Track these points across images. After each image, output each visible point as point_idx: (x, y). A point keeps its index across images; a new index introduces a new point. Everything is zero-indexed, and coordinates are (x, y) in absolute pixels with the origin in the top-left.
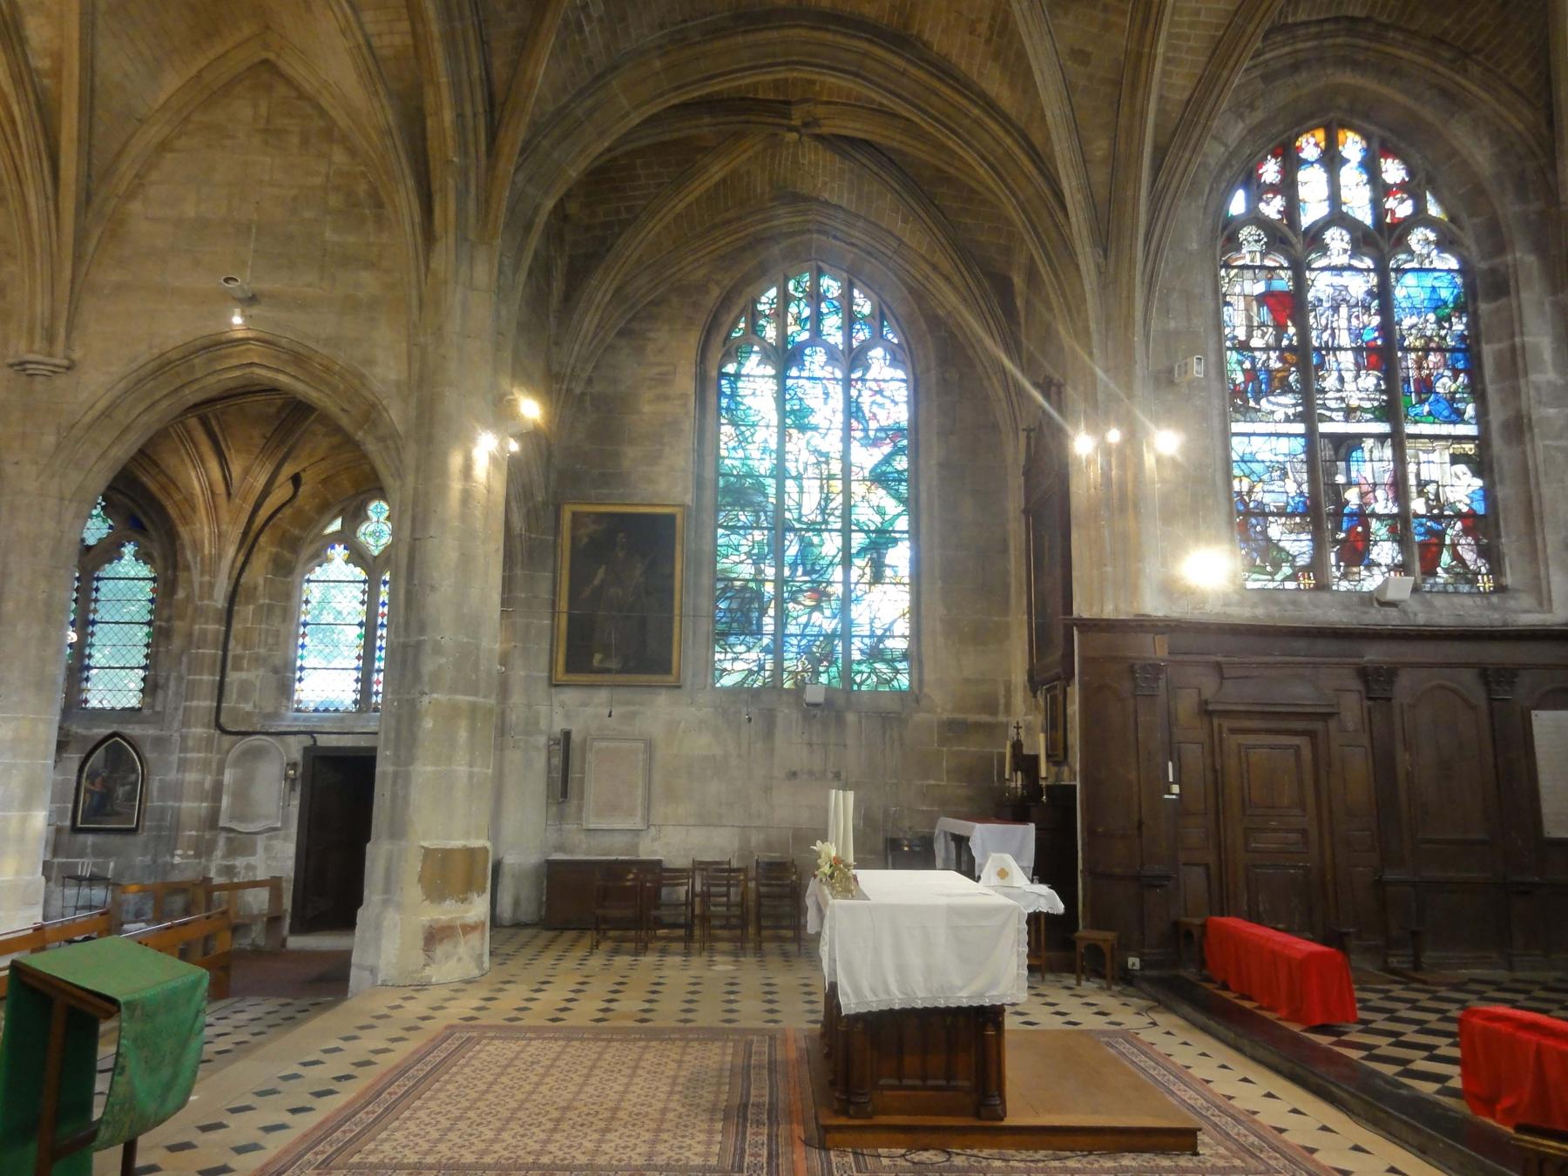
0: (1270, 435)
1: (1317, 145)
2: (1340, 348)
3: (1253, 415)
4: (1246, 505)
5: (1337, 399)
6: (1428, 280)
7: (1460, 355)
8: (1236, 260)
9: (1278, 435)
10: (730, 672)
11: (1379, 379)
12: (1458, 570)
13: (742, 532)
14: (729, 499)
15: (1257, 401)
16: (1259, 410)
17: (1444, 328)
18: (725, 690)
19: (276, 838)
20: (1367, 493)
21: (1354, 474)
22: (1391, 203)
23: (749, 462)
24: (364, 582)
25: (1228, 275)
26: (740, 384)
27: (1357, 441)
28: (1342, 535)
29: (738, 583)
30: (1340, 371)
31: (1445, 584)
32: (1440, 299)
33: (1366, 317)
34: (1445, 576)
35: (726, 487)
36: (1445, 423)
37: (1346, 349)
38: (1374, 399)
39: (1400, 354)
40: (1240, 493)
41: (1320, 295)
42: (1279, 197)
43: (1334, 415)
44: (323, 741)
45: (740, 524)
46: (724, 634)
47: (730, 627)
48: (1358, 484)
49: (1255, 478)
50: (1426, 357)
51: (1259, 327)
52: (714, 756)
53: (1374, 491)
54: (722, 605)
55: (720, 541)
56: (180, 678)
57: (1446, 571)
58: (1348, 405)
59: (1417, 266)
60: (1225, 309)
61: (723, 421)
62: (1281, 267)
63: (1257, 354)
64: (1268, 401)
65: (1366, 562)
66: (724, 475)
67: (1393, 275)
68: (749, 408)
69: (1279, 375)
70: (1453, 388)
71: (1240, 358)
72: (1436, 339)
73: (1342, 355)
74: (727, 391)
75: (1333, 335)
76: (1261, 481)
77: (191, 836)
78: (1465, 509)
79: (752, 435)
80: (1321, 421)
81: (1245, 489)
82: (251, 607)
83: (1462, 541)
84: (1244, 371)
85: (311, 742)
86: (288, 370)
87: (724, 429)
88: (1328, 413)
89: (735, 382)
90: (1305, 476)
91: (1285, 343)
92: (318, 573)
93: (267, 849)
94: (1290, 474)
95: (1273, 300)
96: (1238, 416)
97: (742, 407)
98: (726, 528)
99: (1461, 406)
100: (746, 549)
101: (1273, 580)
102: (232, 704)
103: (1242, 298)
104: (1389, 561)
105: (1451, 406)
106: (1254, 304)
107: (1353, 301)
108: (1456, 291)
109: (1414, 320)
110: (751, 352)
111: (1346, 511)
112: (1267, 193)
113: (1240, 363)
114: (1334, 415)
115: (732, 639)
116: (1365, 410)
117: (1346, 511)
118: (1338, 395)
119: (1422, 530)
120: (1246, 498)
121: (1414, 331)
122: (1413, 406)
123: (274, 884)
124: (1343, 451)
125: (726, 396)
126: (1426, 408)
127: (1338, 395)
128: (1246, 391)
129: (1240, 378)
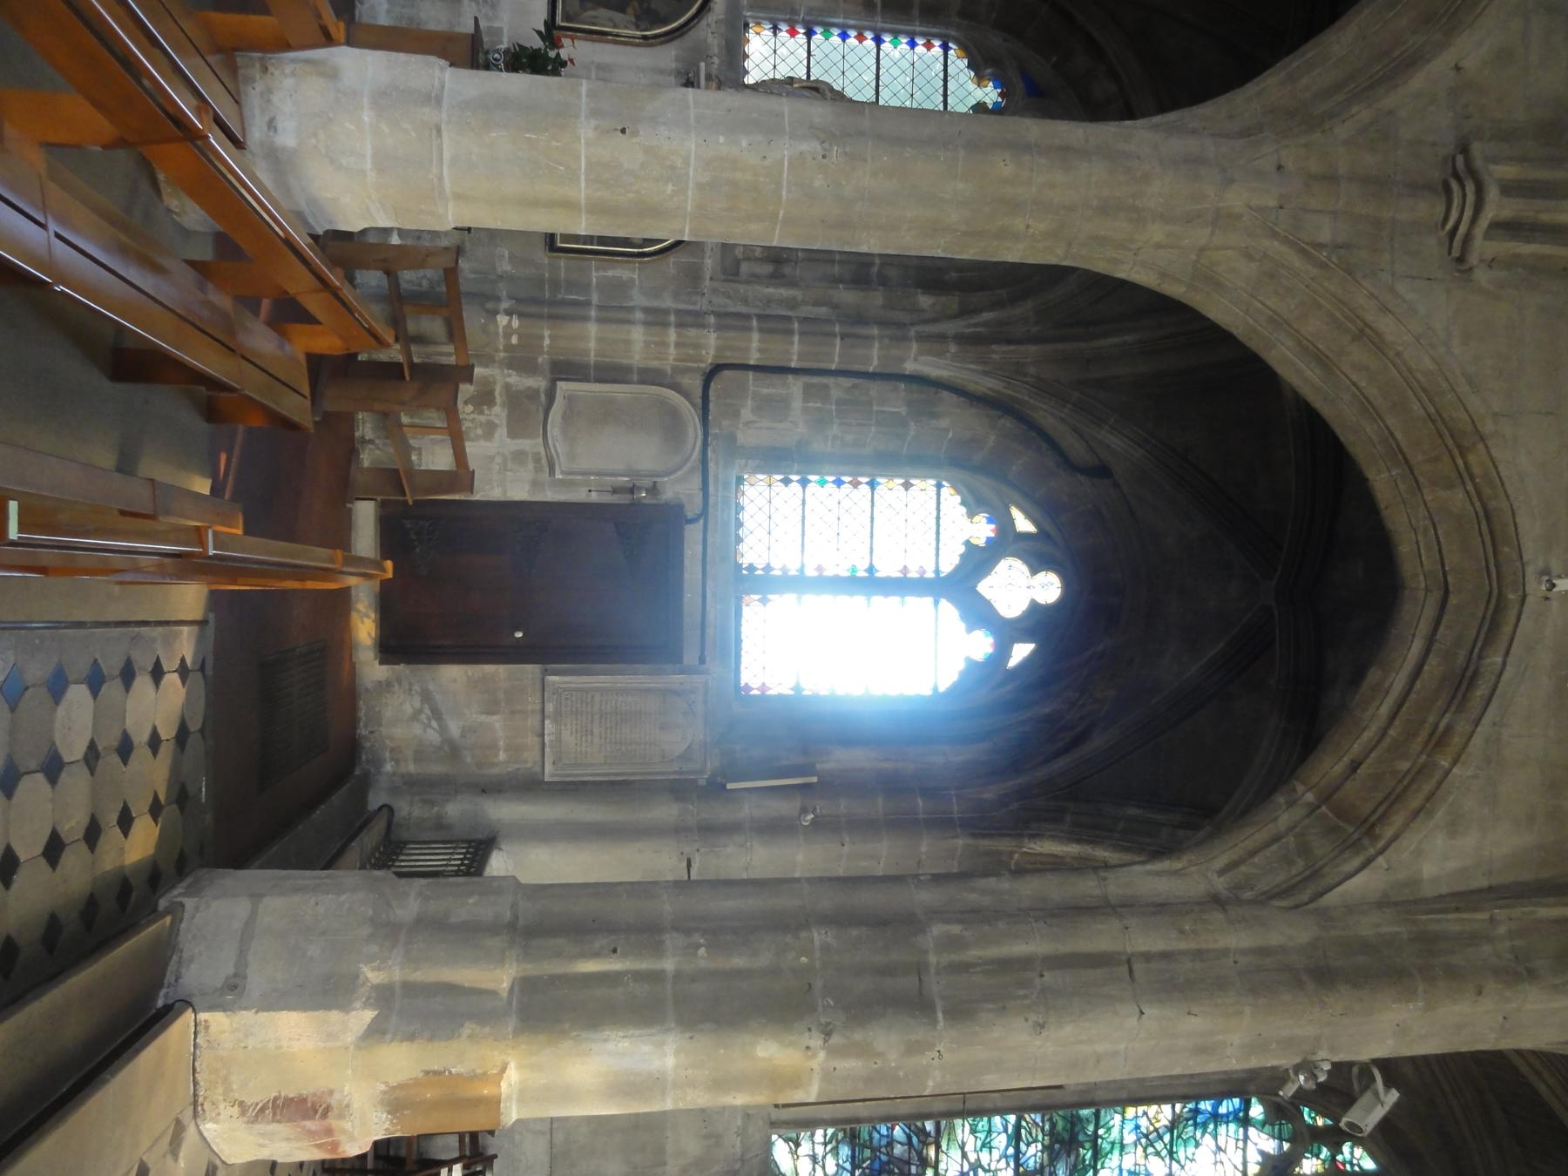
10: (794, 1153)
13: (1011, 1151)
14: (1060, 1124)
18: (769, 1145)
19: (538, 470)
23: (1116, 1152)
24: (937, 571)
26: (1232, 1126)
29: (932, 1152)
35: (1080, 1119)
44: (693, 533)
45: (1023, 1147)
46: (853, 1138)
47: (864, 1146)
52: (665, 1164)
54: (898, 1132)
55: (997, 1120)
56: (793, 304)
61: (1178, 1107)
66: (1097, 1115)
68: (1197, 1145)
74: (1223, 1110)
77: (542, 338)
79: (1158, 1154)
82: (903, 410)
85: (690, 515)
86: (1433, 661)
87: (1167, 1109)
89: (1237, 1119)
92: (951, 500)
93: (519, 457)
97: (1198, 1134)
98: (1018, 1127)
100: (985, 1162)
102: (751, 388)
110: (1281, 1139)
115: (845, 1151)
123: (461, 476)
125: (1215, 1108)
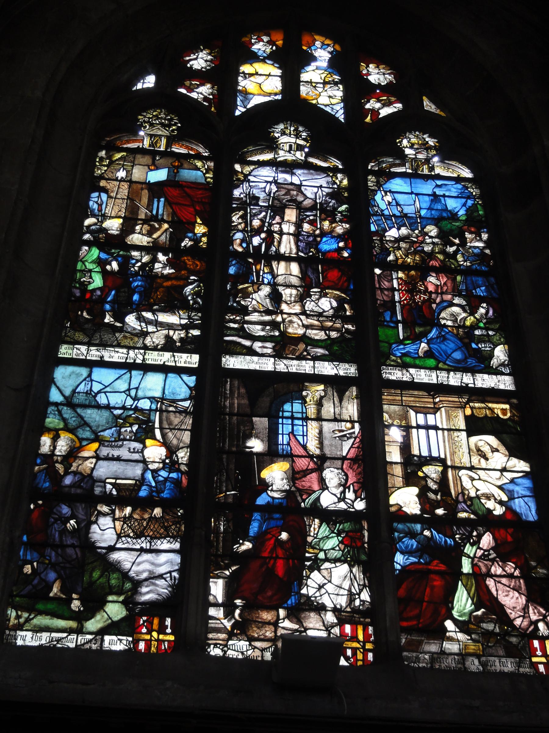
0: (129, 367)
1: (271, 43)
2: (280, 257)
3: (107, 337)
4: (57, 478)
5: (264, 324)
6: (427, 188)
7: (480, 280)
8: (128, 142)
9: (146, 368)
11: (340, 301)
12: (490, 627)
15: (120, 317)
16: (121, 330)
17: (452, 244)
20: (306, 472)
21: (283, 439)
22: (372, 104)
25: (109, 157)
27: (293, 387)
28: (248, 545)
30: (274, 286)
31: (463, 655)
32: (446, 209)
33: (326, 224)
34: (461, 636)
36: (456, 370)
37: (288, 259)
38: (331, 329)
39: (378, 271)
40: (50, 458)
41: (256, 192)
42: (209, 86)
43: (257, 346)
48: (289, 456)
49: (87, 434)
50: (424, 278)
51: (145, 221)
53: (320, 469)
57: (462, 626)
58: (284, 334)
59: (410, 171)
60: (96, 194)
62: (198, 156)
63: (135, 254)
64: (140, 318)
65: (292, 601)
67: (371, 179)
69: (168, 284)
70: (470, 321)
71: (103, 256)
72: (441, 257)
73: (281, 268)
75: (269, 240)
76: (97, 439)
78: (499, 511)
80: (233, 353)
81: (62, 446)
83: (496, 570)
84: (105, 274)
88: (247, 343)
90: (186, 437)
91: (186, 243)
94: (158, 433)
95: (173, 192)
96: (79, 336)
99: (484, 347)
101: (79, 631)
103: (125, 186)
104: (342, 601)
105: (467, 346)
106: (145, 194)
107: (307, 203)
108: (470, 203)
109: (404, 231)
111: (262, 500)
112: (191, 78)
113: (101, 263)
114: (257, 346)
116: (316, 343)
117: (262, 500)
118: (267, 318)
119: (413, 543)
120: (60, 468)
121: (403, 245)
122: (401, 342)
124: (265, 402)
126: (424, 346)
127: (267, 318)
128: (102, 300)
129: (97, 281)
